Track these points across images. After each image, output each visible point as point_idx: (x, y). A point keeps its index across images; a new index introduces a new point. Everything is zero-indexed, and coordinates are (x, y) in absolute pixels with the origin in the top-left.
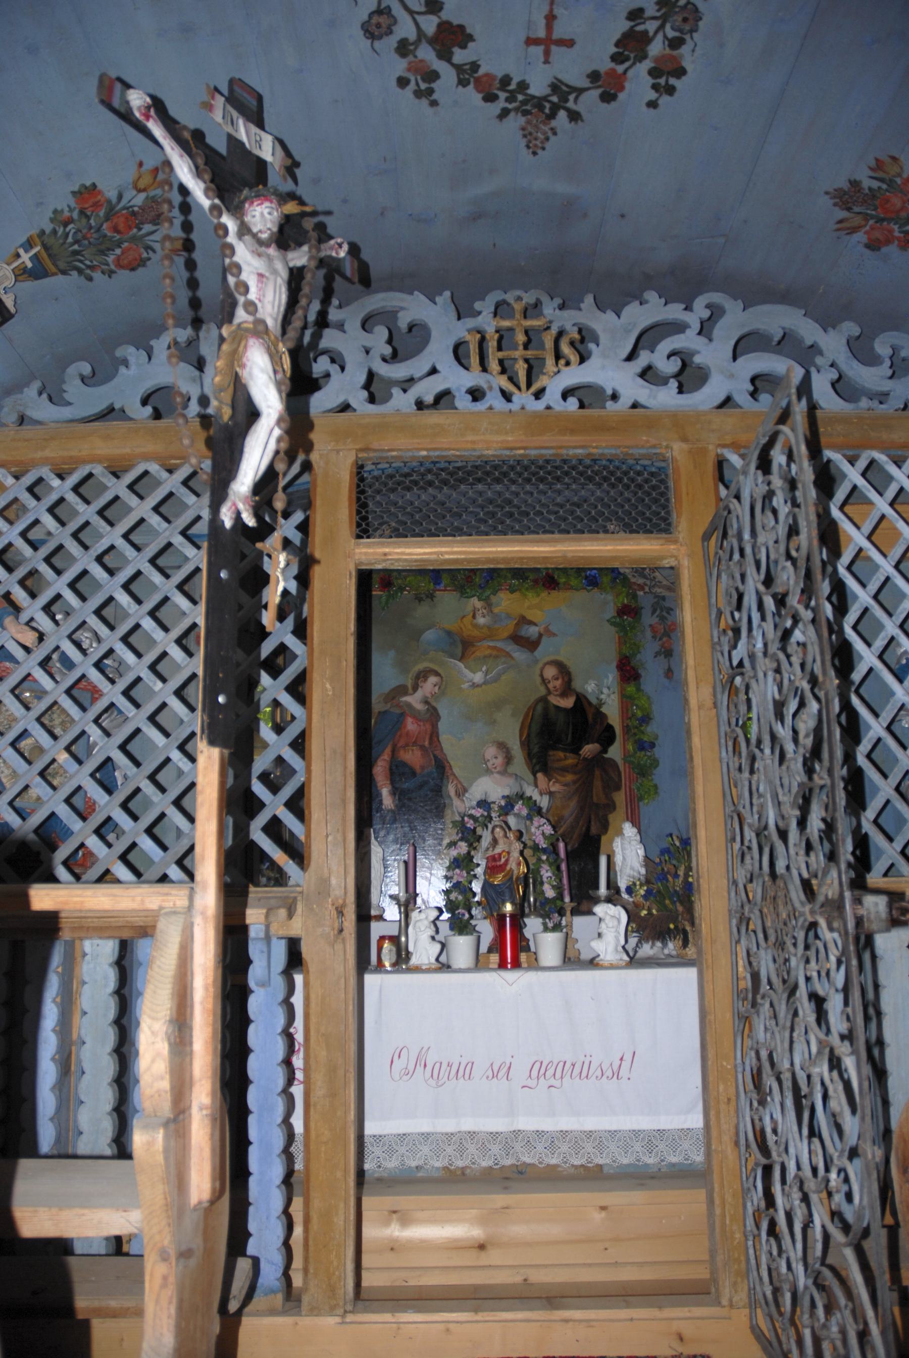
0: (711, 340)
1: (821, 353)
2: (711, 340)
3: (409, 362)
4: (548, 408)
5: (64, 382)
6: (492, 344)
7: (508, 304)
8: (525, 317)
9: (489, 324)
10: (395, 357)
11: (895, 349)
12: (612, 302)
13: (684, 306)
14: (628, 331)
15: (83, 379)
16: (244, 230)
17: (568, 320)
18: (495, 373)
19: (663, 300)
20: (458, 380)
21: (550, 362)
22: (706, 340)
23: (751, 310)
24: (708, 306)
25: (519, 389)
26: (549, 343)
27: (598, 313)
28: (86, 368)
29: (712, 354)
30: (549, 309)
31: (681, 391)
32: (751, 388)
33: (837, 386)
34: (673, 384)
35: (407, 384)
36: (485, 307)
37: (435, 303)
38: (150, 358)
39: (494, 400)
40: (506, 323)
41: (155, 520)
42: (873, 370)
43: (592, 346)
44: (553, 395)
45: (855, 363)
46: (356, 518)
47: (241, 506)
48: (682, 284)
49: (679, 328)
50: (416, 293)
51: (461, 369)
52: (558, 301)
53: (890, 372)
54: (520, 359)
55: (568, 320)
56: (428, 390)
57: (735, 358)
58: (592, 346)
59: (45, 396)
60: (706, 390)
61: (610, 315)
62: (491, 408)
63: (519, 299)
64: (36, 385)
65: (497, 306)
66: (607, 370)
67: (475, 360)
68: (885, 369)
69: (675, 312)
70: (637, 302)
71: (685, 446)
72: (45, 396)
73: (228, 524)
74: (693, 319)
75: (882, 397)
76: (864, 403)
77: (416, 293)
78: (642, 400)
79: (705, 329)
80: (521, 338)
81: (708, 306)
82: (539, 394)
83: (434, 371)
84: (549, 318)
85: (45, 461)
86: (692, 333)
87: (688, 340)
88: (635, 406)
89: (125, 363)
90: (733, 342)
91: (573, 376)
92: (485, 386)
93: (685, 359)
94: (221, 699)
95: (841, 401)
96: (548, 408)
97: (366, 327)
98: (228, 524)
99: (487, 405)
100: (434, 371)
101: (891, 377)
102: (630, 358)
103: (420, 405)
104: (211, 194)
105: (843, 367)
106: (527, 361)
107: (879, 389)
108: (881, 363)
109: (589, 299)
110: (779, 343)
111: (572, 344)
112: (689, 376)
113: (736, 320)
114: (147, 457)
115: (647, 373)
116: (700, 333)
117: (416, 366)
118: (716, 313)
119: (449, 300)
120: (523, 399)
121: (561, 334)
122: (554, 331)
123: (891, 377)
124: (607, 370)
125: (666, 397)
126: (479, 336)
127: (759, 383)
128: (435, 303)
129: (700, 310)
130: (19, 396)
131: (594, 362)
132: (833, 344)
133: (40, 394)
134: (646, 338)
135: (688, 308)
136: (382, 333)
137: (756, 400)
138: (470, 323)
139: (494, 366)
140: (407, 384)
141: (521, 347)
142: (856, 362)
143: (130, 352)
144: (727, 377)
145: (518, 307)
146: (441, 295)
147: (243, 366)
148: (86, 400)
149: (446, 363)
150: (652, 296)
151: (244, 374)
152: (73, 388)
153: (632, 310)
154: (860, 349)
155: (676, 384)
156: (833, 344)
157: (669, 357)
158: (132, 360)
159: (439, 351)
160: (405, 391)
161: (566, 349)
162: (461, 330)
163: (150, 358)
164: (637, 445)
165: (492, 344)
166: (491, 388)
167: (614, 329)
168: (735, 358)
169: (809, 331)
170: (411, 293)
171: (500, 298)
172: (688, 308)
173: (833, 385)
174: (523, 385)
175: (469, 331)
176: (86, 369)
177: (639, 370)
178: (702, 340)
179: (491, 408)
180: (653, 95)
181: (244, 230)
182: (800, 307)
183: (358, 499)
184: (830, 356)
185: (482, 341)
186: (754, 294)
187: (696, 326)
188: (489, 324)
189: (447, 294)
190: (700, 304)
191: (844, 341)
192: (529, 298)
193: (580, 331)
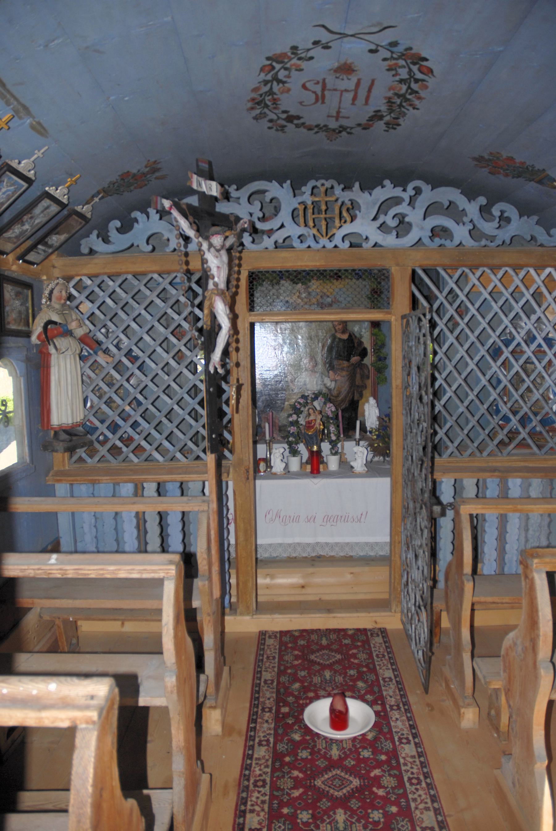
0: (414, 208)
1: (466, 215)
2: (414, 208)
3: (271, 221)
4: (336, 246)
5: (108, 231)
6: (310, 211)
7: (318, 188)
8: (326, 195)
9: (308, 198)
10: (263, 219)
11: (502, 212)
12: (368, 186)
13: (402, 189)
14: (375, 204)
15: (117, 229)
16: (211, 245)
17: (346, 196)
18: (311, 227)
19: (393, 185)
20: (293, 230)
21: (337, 221)
22: (412, 208)
23: (435, 190)
24: (414, 189)
25: (323, 236)
26: (337, 211)
27: (361, 193)
28: (118, 224)
29: (414, 216)
30: (338, 190)
31: (397, 237)
32: (431, 235)
33: (472, 232)
34: (394, 233)
35: (270, 233)
36: (307, 189)
37: (282, 187)
38: (148, 217)
39: (310, 242)
40: (317, 199)
41: (158, 301)
42: (490, 224)
43: (357, 212)
44: (337, 240)
45: (482, 221)
46: (249, 301)
47: (217, 366)
48: (401, 181)
49: (397, 201)
50: (274, 181)
51: (295, 225)
52: (342, 186)
53: (497, 225)
54: (322, 217)
55: (346, 196)
56: (279, 236)
57: (424, 219)
58: (357, 212)
59: (100, 239)
60: (410, 236)
61: (366, 194)
62: (309, 247)
63: (323, 185)
64: (95, 232)
65: (313, 188)
66: (364, 226)
67: (302, 220)
68: (496, 224)
69: (398, 192)
70: (380, 187)
71: (397, 268)
72: (100, 239)
73: (212, 372)
74: (406, 196)
75: (492, 238)
76: (484, 242)
77: (274, 181)
78: (380, 242)
79: (412, 202)
80: (324, 207)
81: (414, 189)
82: (331, 239)
83: (282, 226)
84: (337, 196)
85: (105, 274)
86: (405, 204)
87: (403, 208)
88: (375, 245)
89: (136, 220)
90: (424, 209)
91: (348, 228)
92: (307, 234)
93: (401, 218)
94: (214, 436)
95: (472, 241)
96: (336, 246)
97: (251, 199)
98: (212, 372)
99: (307, 245)
100: (282, 226)
101: (498, 228)
102: (375, 219)
103: (276, 246)
104: (208, 269)
105: (476, 222)
106: (325, 219)
107: (492, 234)
108: (494, 220)
109: (357, 185)
110: (447, 208)
111: (348, 210)
112: (403, 227)
113: (428, 195)
114: (153, 272)
115: (383, 227)
116: (409, 204)
117: (274, 224)
118: (418, 191)
119: (290, 186)
120: (324, 241)
121: (343, 203)
122: (339, 202)
123: (498, 228)
124: (364, 226)
125: (390, 240)
126: (303, 207)
127: (435, 232)
128: (282, 187)
129: (410, 191)
130: (88, 239)
131: (358, 221)
132: (472, 209)
133: (98, 237)
134: (384, 207)
135: (404, 190)
136: (258, 205)
137: (432, 241)
138: (300, 199)
139: (311, 224)
140: (270, 233)
141: (324, 213)
142: (482, 220)
143: (136, 214)
144: (420, 229)
145: (323, 189)
146: (285, 182)
147: (214, 308)
148: (120, 241)
149: (288, 221)
150: (387, 182)
151: (215, 311)
152: (113, 234)
153: (378, 191)
154: (485, 211)
155: (395, 233)
156: (472, 209)
157: (393, 217)
158: (139, 219)
159: (284, 216)
160: (269, 237)
161: (345, 214)
162: (295, 203)
163: (148, 217)
164: (376, 262)
165: (310, 211)
166: (309, 236)
167: (368, 201)
168: (424, 219)
169: (462, 202)
170: (271, 182)
171: (314, 184)
172: (404, 190)
173: (470, 231)
174: (324, 234)
175: (299, 204)
176: (118, 224)
177: (379, 226)
178: (410, 208)
179: (309, 247)
180: (386, 129)
181: (211, 245)
182: (459, 188)
183: (250, 292)
184: (470, 216)
185: (305, 209)
186: (436, 182)
187: (407, 200)
188: (308, 198)
189: (289, 182)
190: (410, 187)
191: (478, 208)
192: (328, 184)
193: (352, 204)
